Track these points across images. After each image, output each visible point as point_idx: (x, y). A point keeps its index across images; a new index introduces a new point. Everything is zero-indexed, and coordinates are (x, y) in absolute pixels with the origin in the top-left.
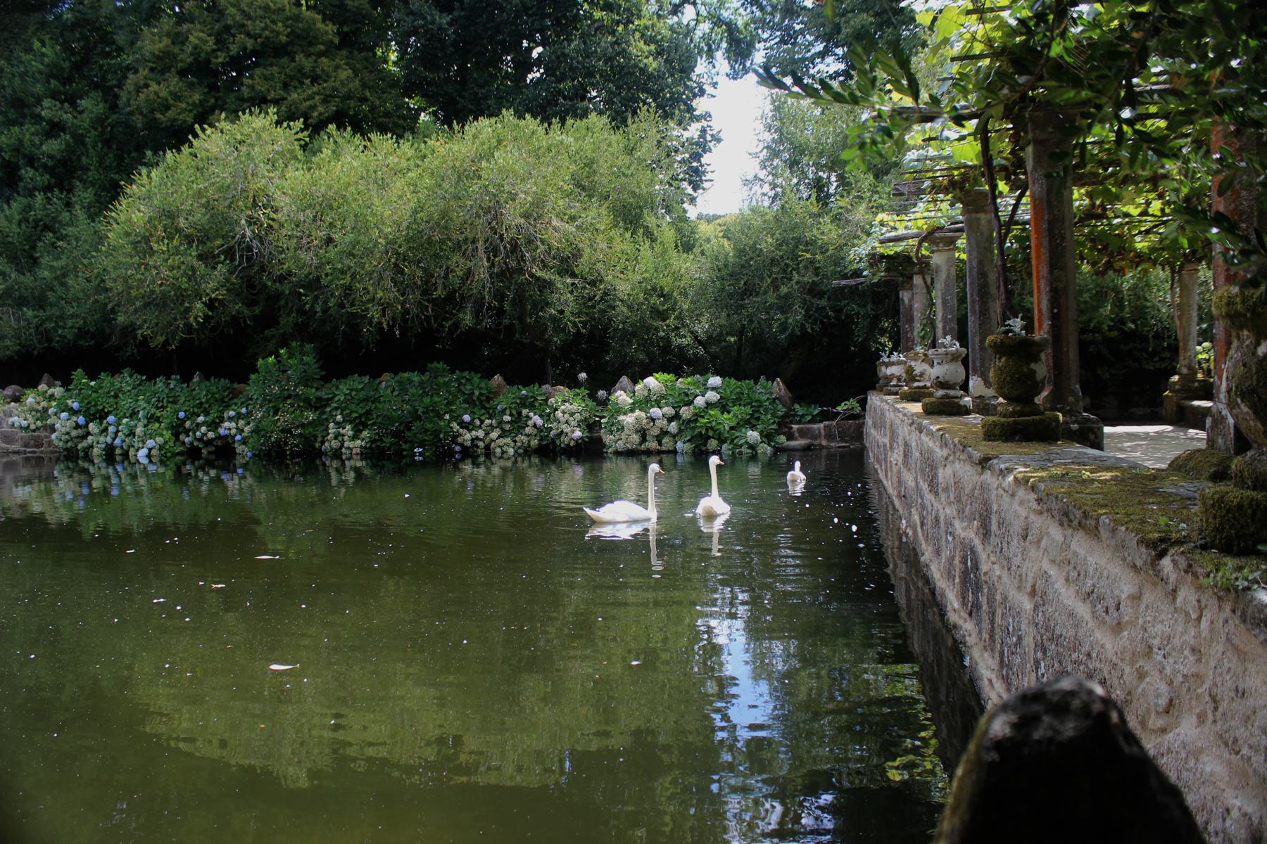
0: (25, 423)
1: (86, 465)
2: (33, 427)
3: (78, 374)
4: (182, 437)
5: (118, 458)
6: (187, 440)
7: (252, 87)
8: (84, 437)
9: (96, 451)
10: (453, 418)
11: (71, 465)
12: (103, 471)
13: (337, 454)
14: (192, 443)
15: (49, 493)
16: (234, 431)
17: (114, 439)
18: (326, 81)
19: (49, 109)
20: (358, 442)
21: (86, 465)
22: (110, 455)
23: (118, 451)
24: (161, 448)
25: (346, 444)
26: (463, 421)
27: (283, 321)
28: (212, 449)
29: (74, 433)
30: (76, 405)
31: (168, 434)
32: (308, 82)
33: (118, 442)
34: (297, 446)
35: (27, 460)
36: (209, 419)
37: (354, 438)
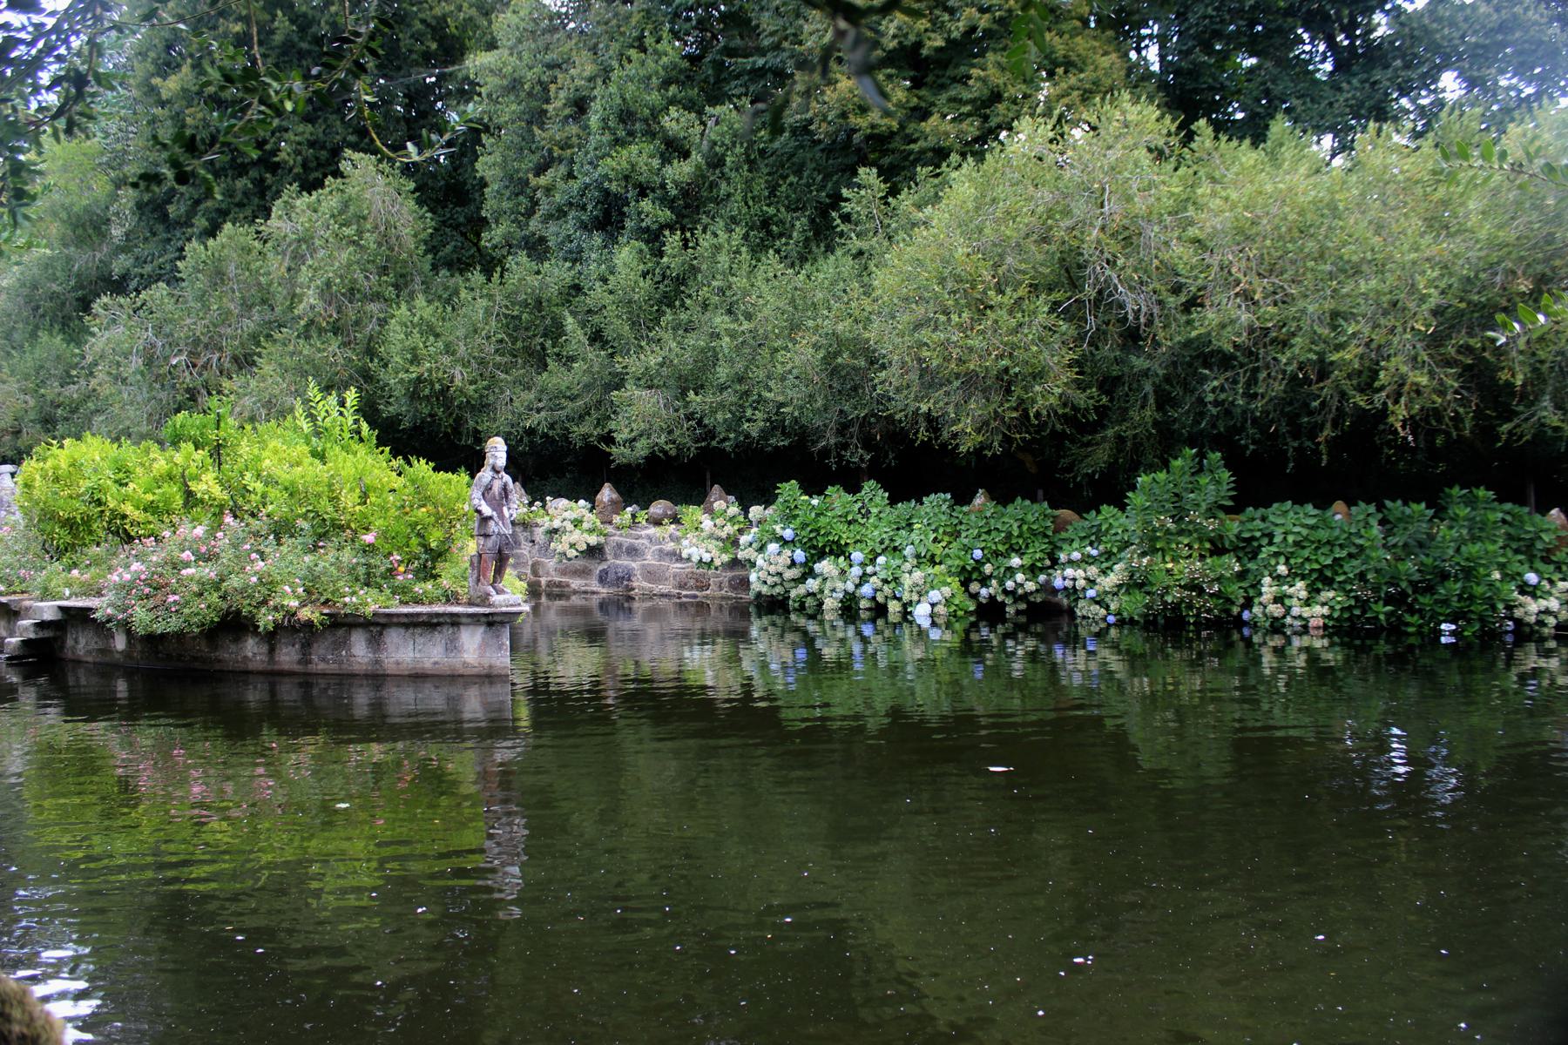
0: (707, 557)
1: (802, 622)
2: (717, 562)
3: (789, 490)
4: (974, 587)
5: (864, 615)
6: (984, 592)
7: (984, 80)
8: (802, 579)
9: (830, 603)
10: (1507, 577)
11: (779, 621)
12: (840, 635)
13: (1277, 626)
14: (992, 598)
15: (734, 659)
16: (1081, 583)
17: (858, 586)
18: (1082, 71)
19: (674, 121)
20: (1318, 610)
21: (802, 622)
22: (849, 609)
23: (864, 604)
24: (948, 602)
25: (1296, 611)
26: (1526, 584)
27: (1134, 414)
28: (1023, 606)
29: (789, 574)
30: (788, 534)
31: (955, 583)
32: (1060, 71)
33: (866, 590)
34: (1209, 611)
35: (682, 606)
36: (1027, 561)
37: (1307, 603)
